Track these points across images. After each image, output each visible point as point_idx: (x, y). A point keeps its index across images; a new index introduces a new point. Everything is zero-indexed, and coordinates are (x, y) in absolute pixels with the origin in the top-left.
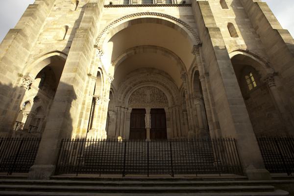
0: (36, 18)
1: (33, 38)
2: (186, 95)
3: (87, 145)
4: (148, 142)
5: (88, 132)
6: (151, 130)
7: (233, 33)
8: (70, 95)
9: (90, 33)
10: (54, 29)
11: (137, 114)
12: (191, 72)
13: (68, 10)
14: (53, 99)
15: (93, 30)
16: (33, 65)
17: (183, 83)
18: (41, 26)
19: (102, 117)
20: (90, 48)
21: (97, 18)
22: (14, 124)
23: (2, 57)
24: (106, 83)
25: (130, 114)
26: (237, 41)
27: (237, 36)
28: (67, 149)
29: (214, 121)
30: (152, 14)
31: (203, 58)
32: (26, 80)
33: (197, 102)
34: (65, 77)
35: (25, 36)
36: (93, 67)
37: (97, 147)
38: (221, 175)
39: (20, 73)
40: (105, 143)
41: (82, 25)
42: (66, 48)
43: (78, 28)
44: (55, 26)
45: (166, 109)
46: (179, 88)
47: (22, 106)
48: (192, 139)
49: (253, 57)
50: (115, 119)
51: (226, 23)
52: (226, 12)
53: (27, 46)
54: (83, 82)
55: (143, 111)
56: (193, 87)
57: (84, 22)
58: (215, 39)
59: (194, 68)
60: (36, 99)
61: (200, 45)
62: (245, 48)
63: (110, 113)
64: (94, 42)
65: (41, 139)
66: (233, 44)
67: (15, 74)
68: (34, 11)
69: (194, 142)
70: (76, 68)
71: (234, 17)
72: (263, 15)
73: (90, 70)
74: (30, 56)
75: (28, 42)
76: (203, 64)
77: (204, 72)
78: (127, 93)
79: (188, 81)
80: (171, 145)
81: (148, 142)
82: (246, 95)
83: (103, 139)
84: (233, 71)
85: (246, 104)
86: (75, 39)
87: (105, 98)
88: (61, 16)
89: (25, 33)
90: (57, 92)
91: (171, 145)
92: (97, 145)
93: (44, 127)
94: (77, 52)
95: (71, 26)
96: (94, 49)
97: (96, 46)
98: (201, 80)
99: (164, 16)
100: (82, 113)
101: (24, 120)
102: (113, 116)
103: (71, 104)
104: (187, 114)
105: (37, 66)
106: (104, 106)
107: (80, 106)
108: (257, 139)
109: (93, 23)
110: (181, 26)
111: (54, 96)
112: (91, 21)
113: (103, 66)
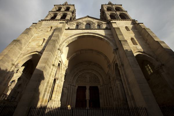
0: (29, 35)
1: (25, 44)
2: (111, 78)
3: (47, 111)
4: (88, 110)
5: (48, 102)
7: (134, 43)
8: (41, 77)
9: (56, 42)
10: (37, 40)
11: (81, 90)
12: (113, 64)
13: (46, 31)
14: (30, 79)
15: (58, 41)
16: (22, 59)
18: (30, 39)
19: (59, 91)
20: (55, 50)
21: (61, 35)
22: (1, 95)
23: (5, 54)
24: (63, 70)
25: (76, 90)
26: (137, 47)
27: (137, 44)
28: (33, 115)
29: (130, 95)
30: (90, 33)
31: (119, 56)
32: (16, 67)
33: (118, 82)
34: (39, 66)
35: (21, 43)
36: (56, 61)
37: (53, 113)
39: (13, 63)
40: (59, 110)
41: (53, 38)
42: (42, 50)
43: (50, 40)
44: (38, 39)
45: (99, 87)
46: (106, 73)
47: (10, 84)
48: (117, 108)
49: (147, 56)
51: (130, 38)
52: (129, 33)
53: (21, 49)
55: (85, 88)
56: (115, 73)
57: (54, 37)
58: (125, 46)
59: (114, 62)
60: (19, 79)
61: (117, 49)
62: (142, 50)
63: (64, 88)
64: (58, 47)
65: (17, 106)
66: (135, 48)
67: (10, 64)
68: (28, 31)
70: (46, 61)
71: (134, 35)
72: (149, 34)
74: (22, 54)
75: (22, 46)
76: (119, 59)
77: (121, 64)
78: (75, 76)
80: (103, 112)
82: (148, 78)
83: (58, 107)
84: (138, 63)
86: (48, 45)
88: (42, 34)
89: (21, 42)
90: (33, 75)
92: (54, 111)
93: (20, 98)
94: (48, 52)
95: (46, 39)
96: (58, 50)
97: (59, 49)
98: (119, 69)
99: (96, 34)
100: (46, 89)
101: (8, 93)
102: (66, 91)
103: (40, 83)
104: (112, 90)
105: (24, 60)
106: (60, 84)
107: (46, 84)
108: (160, 108)
109: (58, 38)
110: (106, 39)
111: (30, 78)
112: (58, 36)
113: (62, 60)
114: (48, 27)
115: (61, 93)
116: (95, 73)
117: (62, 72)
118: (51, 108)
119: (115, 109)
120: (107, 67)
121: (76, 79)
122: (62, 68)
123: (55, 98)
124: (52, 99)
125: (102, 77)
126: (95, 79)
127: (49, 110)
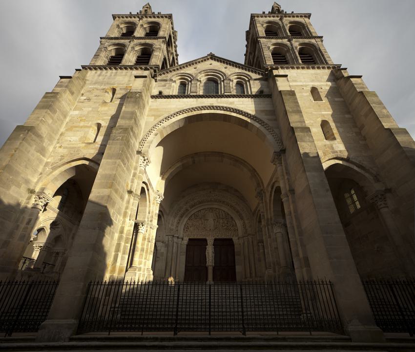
0: (55, 112)
1: (51, 139)
3: (124, 289)
4: (210, 285)
5: (127, 271)
6: (214, 269)
7: (328, 135)
8: (104, 220)
9: (131, 134)
10: (82, 127)
11: (196, 246)
12: (270, 189)
13: (101, 101)
14: (78, 225)
15: (135, 129)
16: (51, 177)
17: (259, 203)
18: (62, 123)
19: (147, 249)
20: (130, 155)
21: (141, 113)
22: (19, 261)
23: (4, 164)
24: (153, 204)
25: (185, 246)
26: (334, 146)
27: (335, 139)
28: (96, 296)
29: (301, 256)
30: (217, 108)
31: (286, 169)
32: (40, 198)
33: (277, 230)
34: (96, 193)
35: (39, 136)
36: (136, 181)
37: (139, 292)
38: (312, 333)
39: (32, 188)
40: (150, 286)
41: (121, 122)
42: (98, 154)
43: (115, 126)
44: (82, 124)
45: (235, 239)
46: (253, 211)
47: (33, 236)
48: (271, 282)
49: (355, 168)
50: (165, 253)
51: (319, 120)
52: (319, 106)
53: (42, 151)
54: (121, 202)
56: (272, 210)
57: (123, 118)
58: (303, 144)
59: (274, 183)
60: (54, 225)
61: (283, 151)
62: (345, 155)
63: (159, 244)
64: (137, 147)
65: (58, 281)
66: (328, 149)
67: (23, 190)
68: (53, 102)
69: (274, 286)
70: (112, 182)
71: (330, 112)
72: (371, 109)
73: (131, 187)
74: (47, 164)
75: (44, 145)
76: (286, 177)
77: (288, 189)
79: (266, 202)
81: (210, 285)
82: (346, 220)
83: (148, 280)
84: (328, 187)
85: (346, 232)
86: (110, 142)
87: (152, 225)
88: (90, 109)
89: (40, 132)
90: (84, 216)
91: (241, 290)
92: (139, 289)
93: (64, 264)
94: (113, 160)
95: (105, 124)
96: (137, 156)
97: (139, 152)
98: (283, 200)
99: (233, 112)
100: (119, 245)
101: (35, 255)
102: (162, 249)
103: (104, 232)
105: (56, 179)
106: (149, 235)
107: (116, 236)
108: (363, 282)
109: (135, 120)
110: (257, 125)
111: (80, 222)
112: (133, 117)
113: (149, 180)
114: (103, 89)
115: (152, 253)
116: (226, 210)
117: (151, 208)
118: (132, 283)
119: (268, 284)
120: (256, 197)
121: (184, 223)
122: (152, 199)
123: (140, 263)
124: (133, 265)
125: (242, 218)
126: (226, 222)
127: (128, 287)
